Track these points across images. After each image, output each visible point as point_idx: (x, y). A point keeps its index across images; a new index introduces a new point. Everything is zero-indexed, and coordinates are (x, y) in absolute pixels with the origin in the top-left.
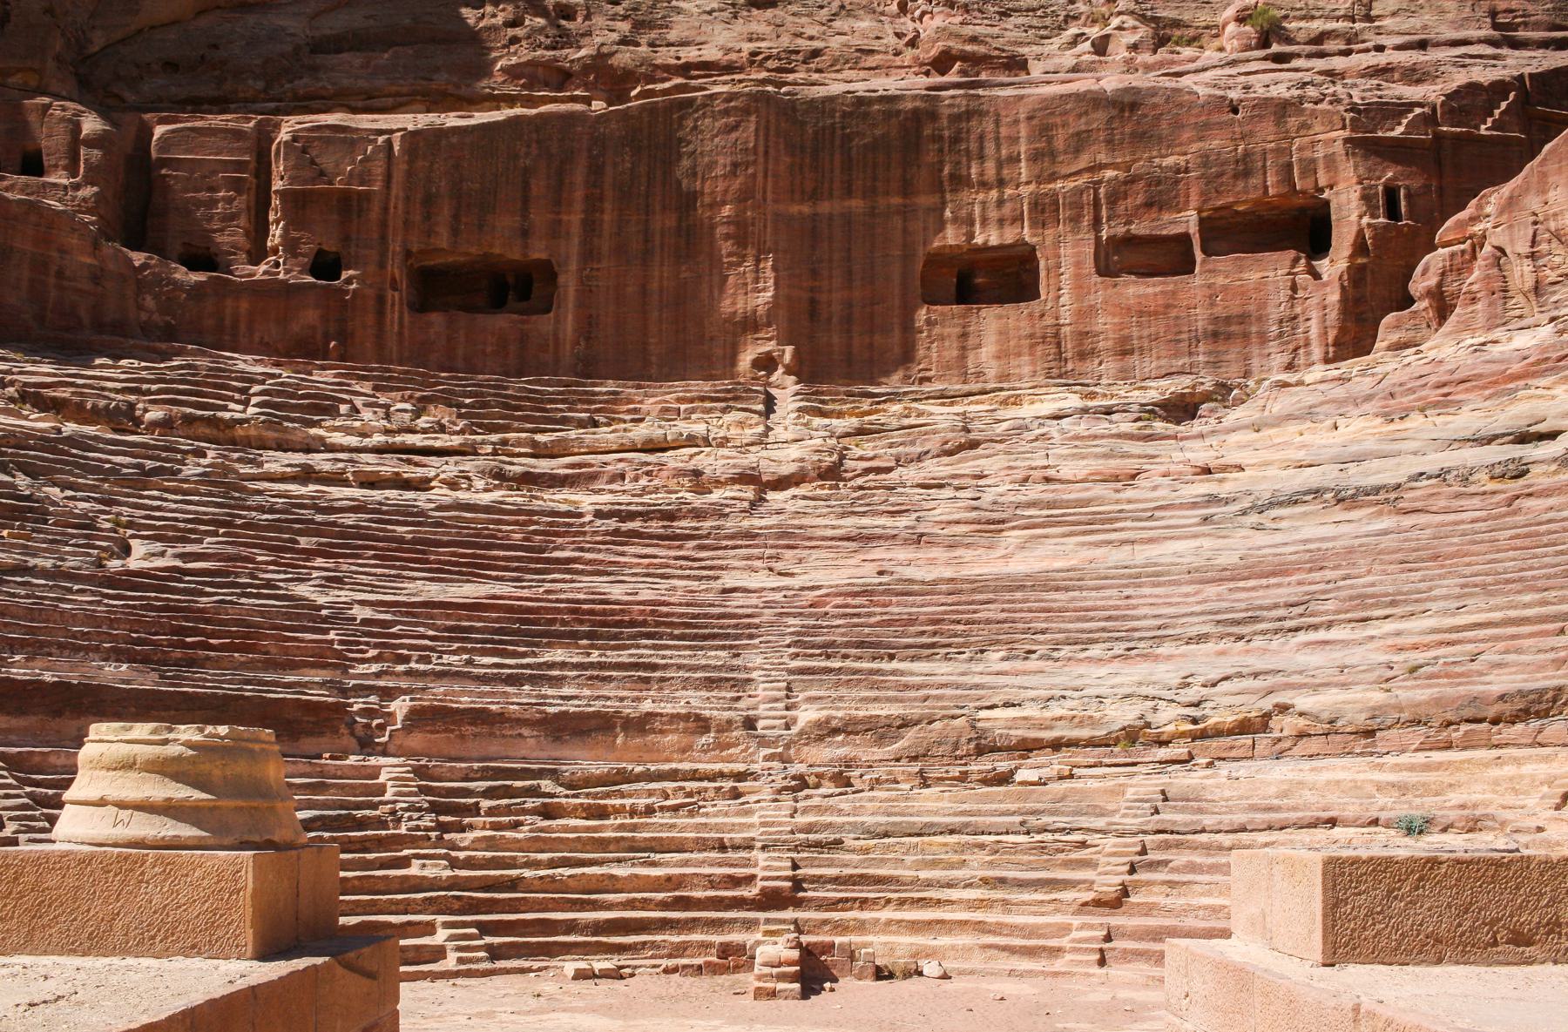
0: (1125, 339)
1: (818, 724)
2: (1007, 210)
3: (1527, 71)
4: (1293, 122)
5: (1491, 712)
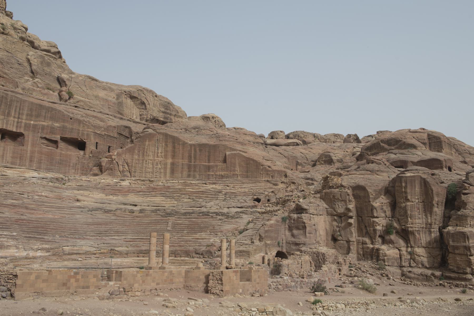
0: (41, 160)
1: (36, 248)
2: (19, 124)
3: (118, 124)
4: (82, 125)
5: (143, 252)
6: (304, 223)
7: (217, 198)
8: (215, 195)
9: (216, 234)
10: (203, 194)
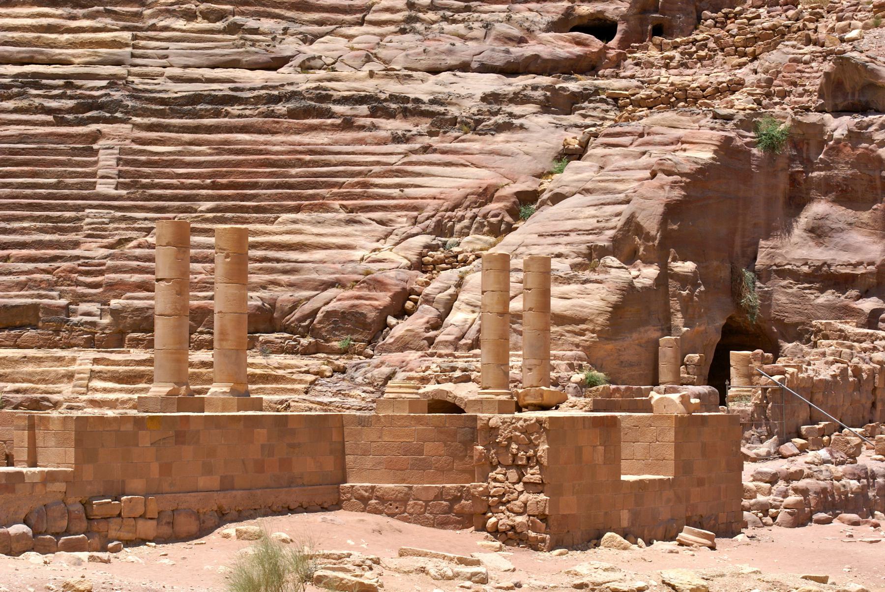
9: (381, 222)
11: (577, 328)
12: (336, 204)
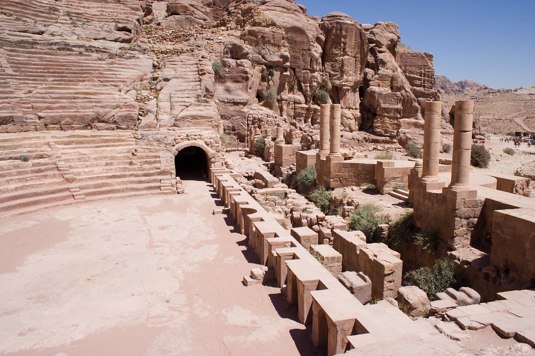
6: (246, 73)
7: (56, 19)
8: (48, 13)
10: (26, 9)
11: (209, 120)
12: (96, 80)
